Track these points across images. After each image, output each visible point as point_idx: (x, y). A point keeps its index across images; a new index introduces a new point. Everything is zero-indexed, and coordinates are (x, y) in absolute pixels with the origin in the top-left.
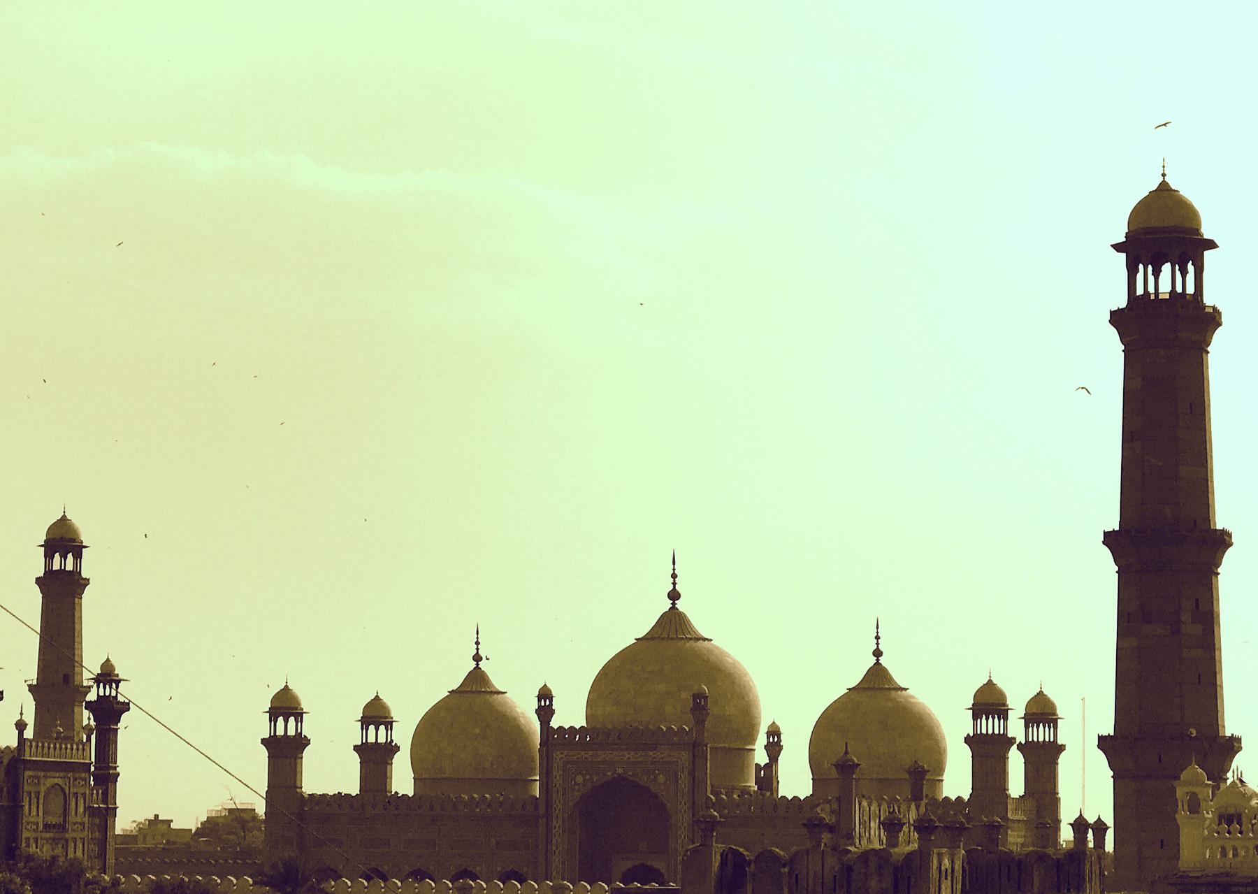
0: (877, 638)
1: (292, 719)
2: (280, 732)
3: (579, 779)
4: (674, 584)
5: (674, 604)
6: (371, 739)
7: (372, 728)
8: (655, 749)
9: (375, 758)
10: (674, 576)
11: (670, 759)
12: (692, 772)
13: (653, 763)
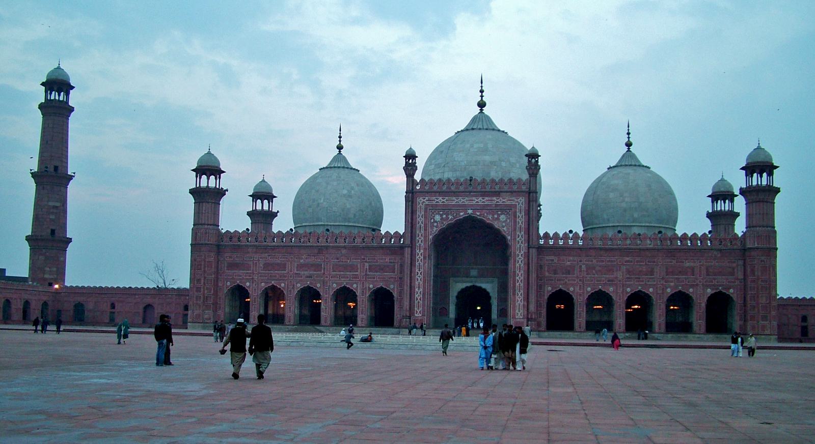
0: (629, 134)
1: (212, 177)
3: (438, 218)
4: (482, 96)
5: (481, 110)
6: (259, 207)
7: (259, 201)
9: (262, 218)
10: (482, 91)
11: (509, 203)
12: (528, 213)
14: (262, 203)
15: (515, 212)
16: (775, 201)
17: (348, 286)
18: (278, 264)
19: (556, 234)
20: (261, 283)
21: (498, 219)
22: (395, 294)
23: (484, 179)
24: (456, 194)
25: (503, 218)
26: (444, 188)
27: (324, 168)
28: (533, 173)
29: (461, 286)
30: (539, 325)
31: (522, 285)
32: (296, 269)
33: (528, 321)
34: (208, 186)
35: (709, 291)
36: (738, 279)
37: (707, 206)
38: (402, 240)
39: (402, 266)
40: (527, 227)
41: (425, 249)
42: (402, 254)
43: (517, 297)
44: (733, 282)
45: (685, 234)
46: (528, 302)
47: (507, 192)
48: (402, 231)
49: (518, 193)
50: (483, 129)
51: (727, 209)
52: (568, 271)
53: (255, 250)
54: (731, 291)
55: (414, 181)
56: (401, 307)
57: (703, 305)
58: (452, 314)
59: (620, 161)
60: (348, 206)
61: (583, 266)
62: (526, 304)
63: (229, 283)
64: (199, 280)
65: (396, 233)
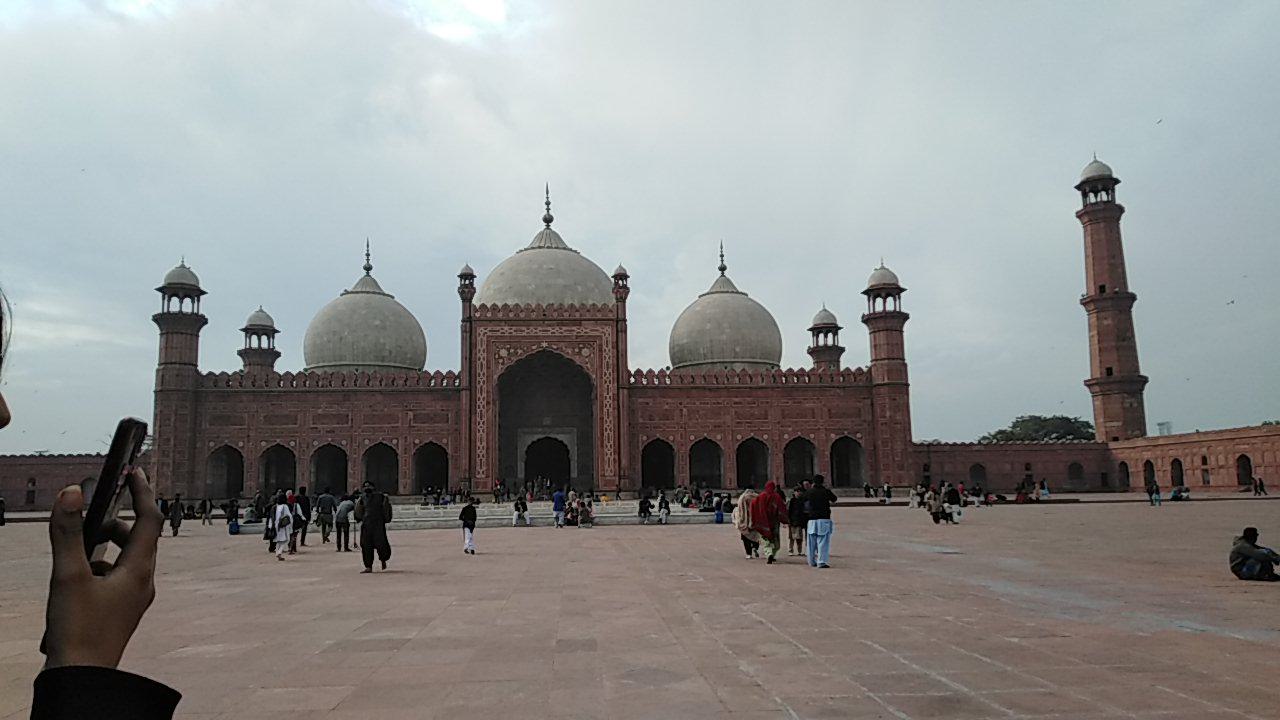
0: (722, 256)
1: (187, 301)
3: (504, 353)
4: (548, 209)
5: (548, 226)
7: (254, 337)
8: (580, 325)
9: (260, 359)
10: (548, 203)
13: (577, 337)
14: (259, 339)
15: (601, 345)
18: (286, 416)
19: (650, 371)
21: (579, 353)
22: (449, 451)
23: (561, 304)
24: (527, 322)
25: (585, 352)
26: (511, 315)
27: (347, 292)
28: (621, 298)
29: (530, 439)
30: (633, 482)
32: (311, 422)
33: (620, 479)
34: (181, 312)
36: (865, 421)
37: (809, 341)
38: (458, 381)
39: (458, 415)
40: (615, 362)
41: (488, 392)
42: (459, 399)
43: (606, 450)
44: (860, 425)
45: (802, 370)
47: (589, 320)
48: (457, 369)
49: (605, 321)
50: (551, 248)
51: (830, 342)
52: (666, 416)
53: (252, 397)
54: (859, 435)
56: (456, 468)
57: (828, 453)
58: (521, 475)
59: (712, 288)
60: (382, 341)
61: (685, 410)
62: (617, 458)
63: (212, 444)
64: (169, 440)
65: (450, 372)
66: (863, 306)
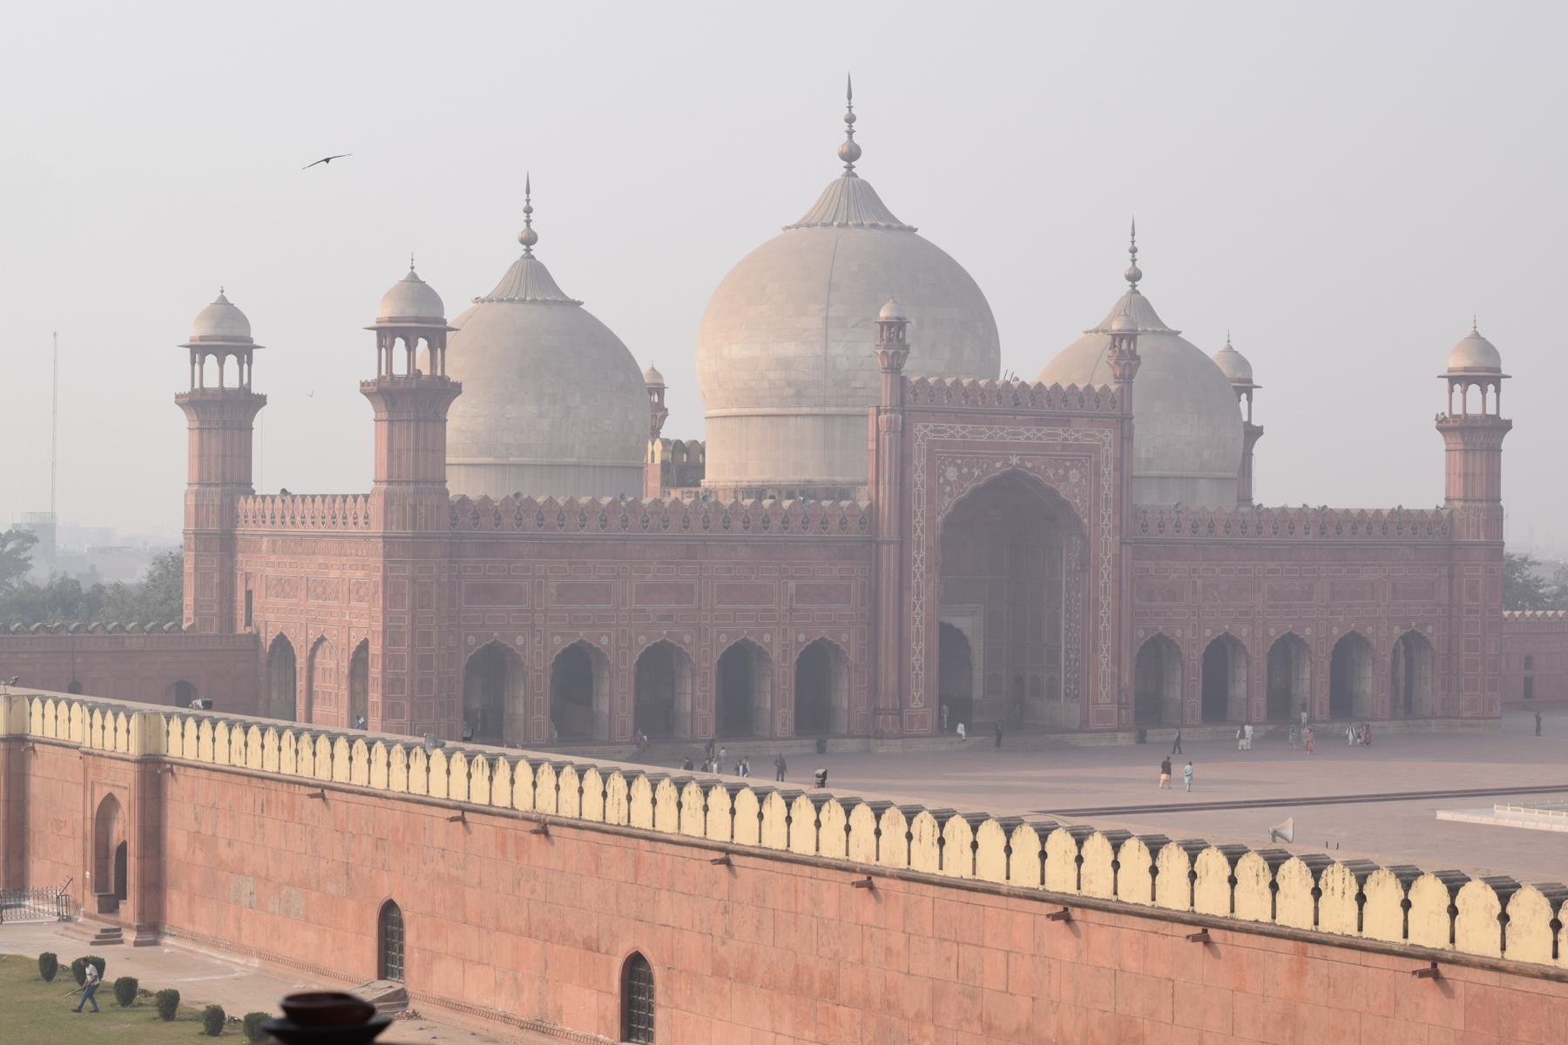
2: (400, 369)
3: (952, 473)
6: (211, 382)
7: (211, 360)
12: (1119, 466)
14: (221, 363)
16: (1503, 446)
17: (752, 639)
20: (553, 635)
31: (1109, 628)
35: (1398, 631)
46: (1119, 666)
54: (1430, 629)
55: (903, 379)
61: (1199, 582)
66: (1439, 400)
